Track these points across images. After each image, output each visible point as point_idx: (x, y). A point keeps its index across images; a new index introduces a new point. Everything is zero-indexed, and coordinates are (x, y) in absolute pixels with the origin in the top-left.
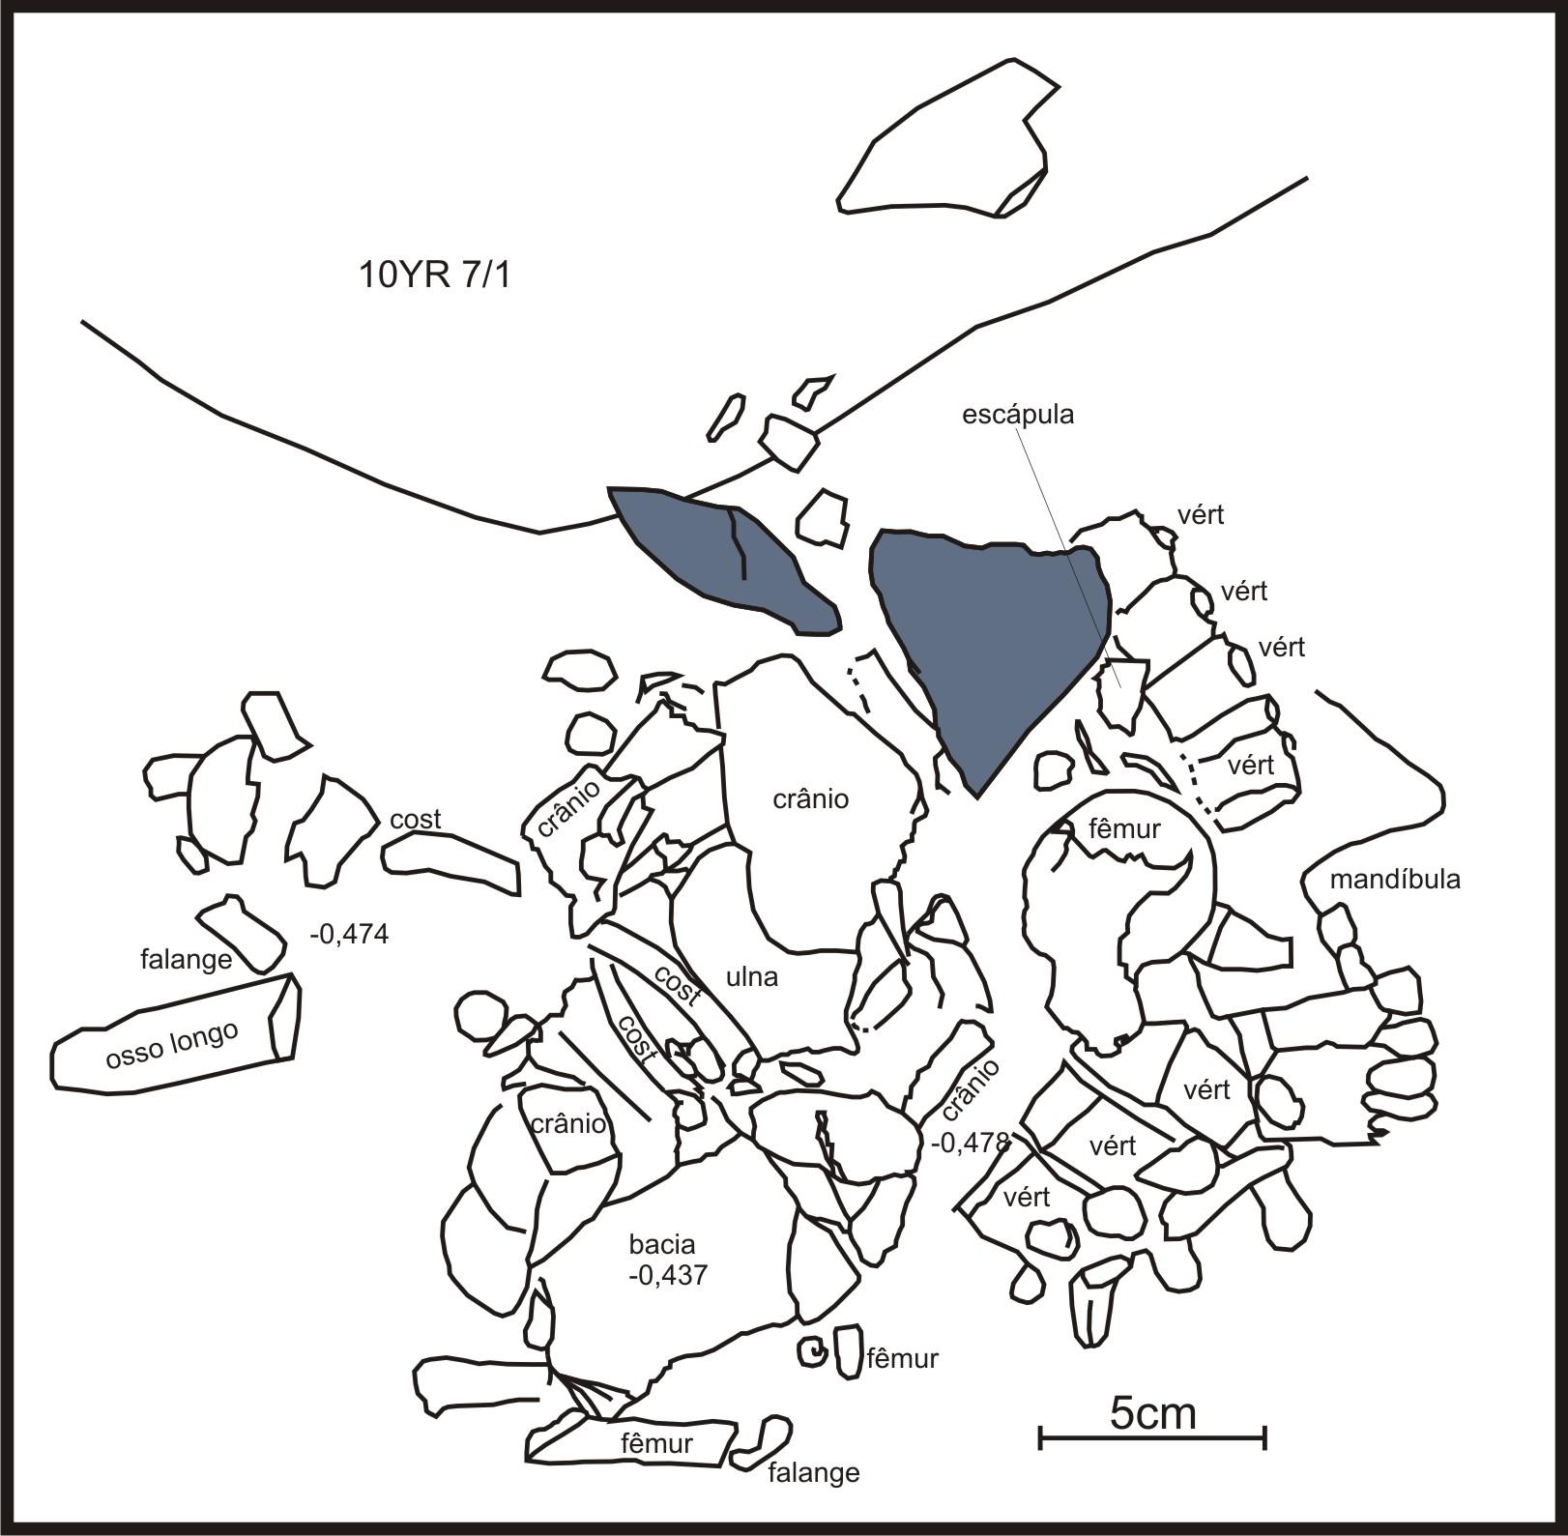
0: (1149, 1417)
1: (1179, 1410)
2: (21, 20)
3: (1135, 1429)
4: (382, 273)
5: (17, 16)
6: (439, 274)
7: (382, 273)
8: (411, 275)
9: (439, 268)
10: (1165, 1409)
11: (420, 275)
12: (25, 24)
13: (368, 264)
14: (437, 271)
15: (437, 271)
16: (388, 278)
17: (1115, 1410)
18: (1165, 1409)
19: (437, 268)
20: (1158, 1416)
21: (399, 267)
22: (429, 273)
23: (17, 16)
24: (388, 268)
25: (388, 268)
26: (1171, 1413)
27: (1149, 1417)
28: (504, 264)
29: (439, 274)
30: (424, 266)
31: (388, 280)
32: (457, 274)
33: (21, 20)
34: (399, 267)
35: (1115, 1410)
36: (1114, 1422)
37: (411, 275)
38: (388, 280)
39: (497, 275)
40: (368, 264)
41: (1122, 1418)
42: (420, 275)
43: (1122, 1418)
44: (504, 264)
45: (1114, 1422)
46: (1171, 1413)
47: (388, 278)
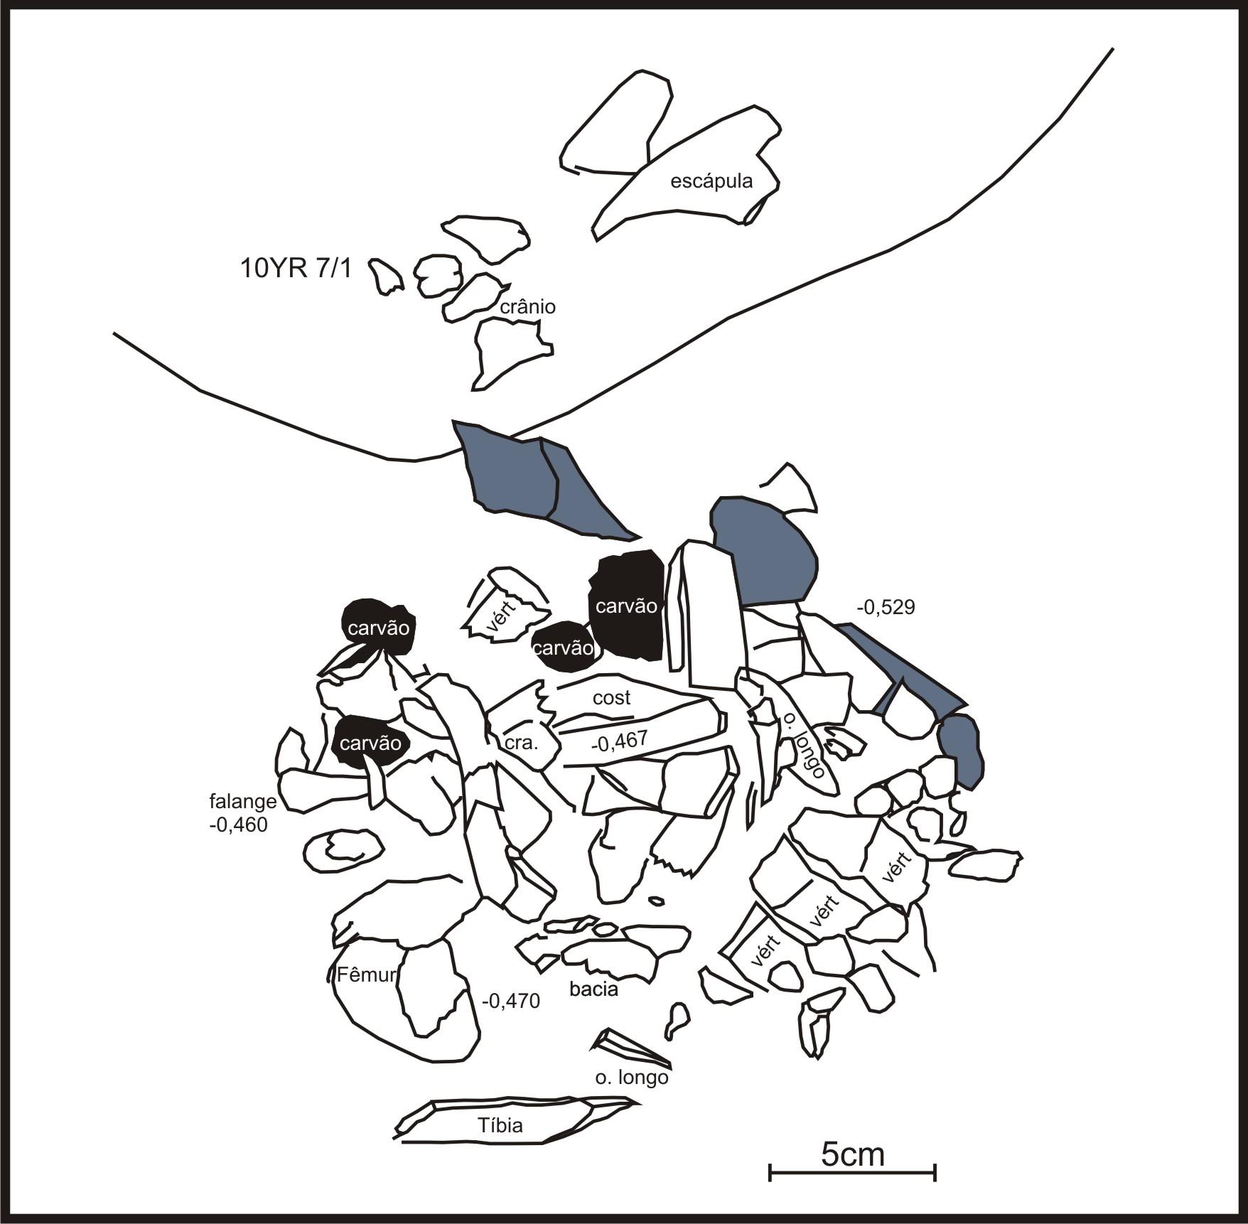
0: (850, 1157)
1: (872, 1152)
2: (15, 15)
3: (840, 1166)
4: (256, 267)
5: (13, 12)
6: (299, 268)
7: (256, 267)
8: (279, 268)
9: (300, 263)
10: (861, 1151)
12: (18, 18)
13: (247, 260)
14: (297, 266)
15: (297, 266)
16: (262, 271)
17: (825, 1152)
18: (861, 1151)
19: (297, 263)
20: (857, 1156)
21: (270, 262)
22: (292, 267)
23: (13, 12)
24: (262, 263)
25: (262, 263)
26: (866, 1154)
27: (850, 1157)
28: (347, 260)
29: (299, 268)
30: (288, 261)
31: (262, 272)
32: (313, 267)
33: (15, 15)
34: (270, 262)
35: (825, 1152)
36: (824, 1161)
37: (279, 268)
38: (262, 272)
39: (341, 268)
40: (247, 260)
41: (830, 1158)
43: (830, 1158)
44: (347, 260)
45: (824, 1161)
46: (866, 1154)
47: (262, 271)
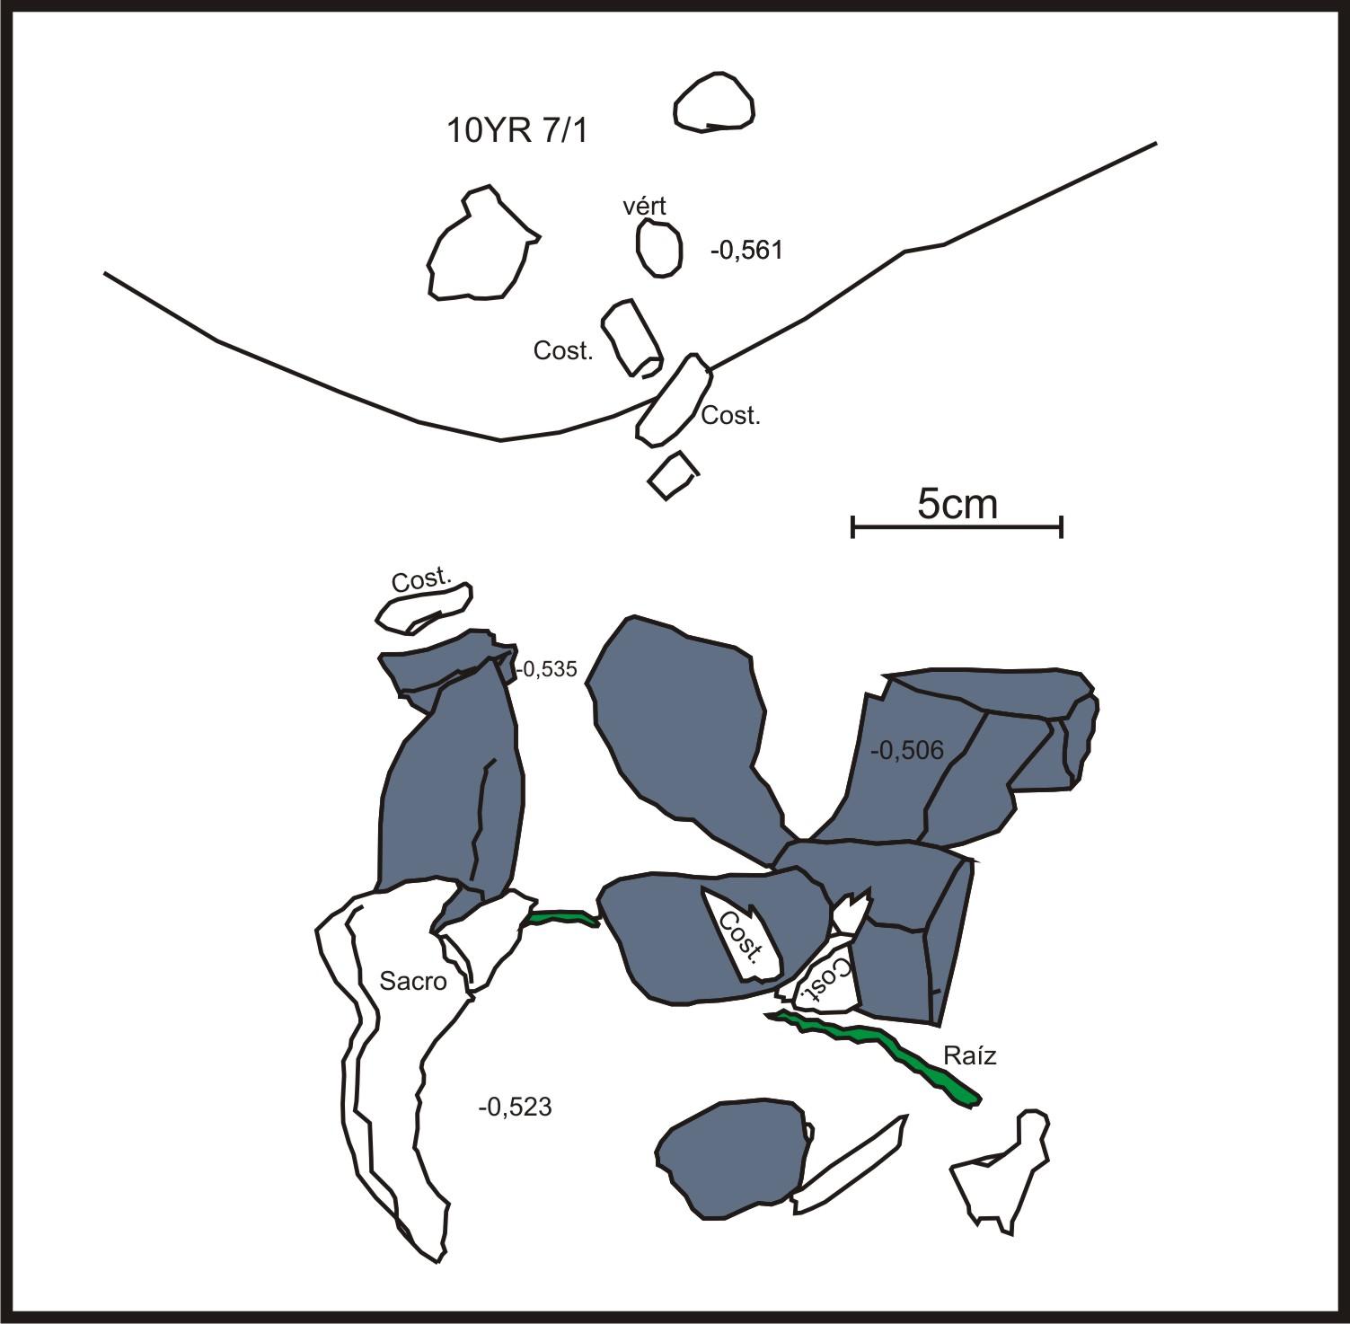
6: (521, 130)
8: (495, 130)
9: (522, 124)
11: (504, 131)
13: (456, 121)
14: (519, 127)
15: (519, 127)
16: (474, 134)
19: (519, 124)
21: (485, 123)
22: (512, 129)
24: (474, 124)
25: (474, 124)
28: (582, 121)
29: (521, 130)
30: (507, 122)
31: (474, 135)
32: (538, 129)
34: (485, 123)
37: (495, 130)
38: (474, 135)
39: (575, 130)
40: (456, 121)
42: (504, 131)
44: (582, 121)
47: (474, 134)
